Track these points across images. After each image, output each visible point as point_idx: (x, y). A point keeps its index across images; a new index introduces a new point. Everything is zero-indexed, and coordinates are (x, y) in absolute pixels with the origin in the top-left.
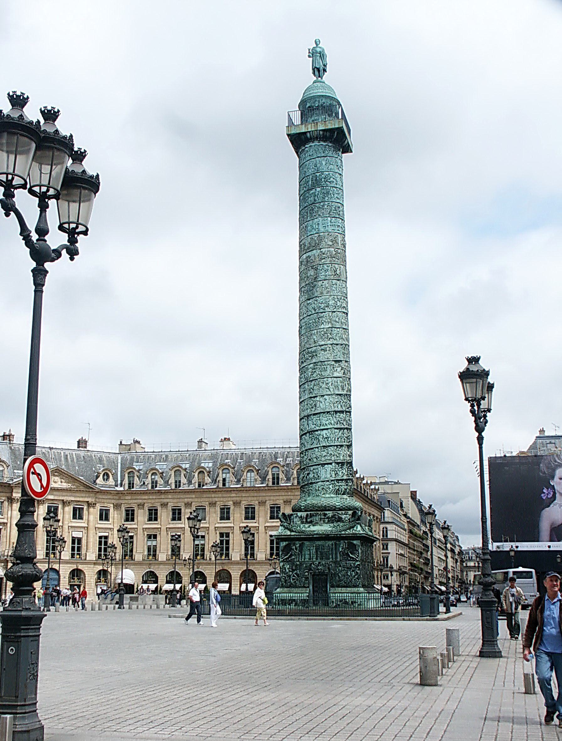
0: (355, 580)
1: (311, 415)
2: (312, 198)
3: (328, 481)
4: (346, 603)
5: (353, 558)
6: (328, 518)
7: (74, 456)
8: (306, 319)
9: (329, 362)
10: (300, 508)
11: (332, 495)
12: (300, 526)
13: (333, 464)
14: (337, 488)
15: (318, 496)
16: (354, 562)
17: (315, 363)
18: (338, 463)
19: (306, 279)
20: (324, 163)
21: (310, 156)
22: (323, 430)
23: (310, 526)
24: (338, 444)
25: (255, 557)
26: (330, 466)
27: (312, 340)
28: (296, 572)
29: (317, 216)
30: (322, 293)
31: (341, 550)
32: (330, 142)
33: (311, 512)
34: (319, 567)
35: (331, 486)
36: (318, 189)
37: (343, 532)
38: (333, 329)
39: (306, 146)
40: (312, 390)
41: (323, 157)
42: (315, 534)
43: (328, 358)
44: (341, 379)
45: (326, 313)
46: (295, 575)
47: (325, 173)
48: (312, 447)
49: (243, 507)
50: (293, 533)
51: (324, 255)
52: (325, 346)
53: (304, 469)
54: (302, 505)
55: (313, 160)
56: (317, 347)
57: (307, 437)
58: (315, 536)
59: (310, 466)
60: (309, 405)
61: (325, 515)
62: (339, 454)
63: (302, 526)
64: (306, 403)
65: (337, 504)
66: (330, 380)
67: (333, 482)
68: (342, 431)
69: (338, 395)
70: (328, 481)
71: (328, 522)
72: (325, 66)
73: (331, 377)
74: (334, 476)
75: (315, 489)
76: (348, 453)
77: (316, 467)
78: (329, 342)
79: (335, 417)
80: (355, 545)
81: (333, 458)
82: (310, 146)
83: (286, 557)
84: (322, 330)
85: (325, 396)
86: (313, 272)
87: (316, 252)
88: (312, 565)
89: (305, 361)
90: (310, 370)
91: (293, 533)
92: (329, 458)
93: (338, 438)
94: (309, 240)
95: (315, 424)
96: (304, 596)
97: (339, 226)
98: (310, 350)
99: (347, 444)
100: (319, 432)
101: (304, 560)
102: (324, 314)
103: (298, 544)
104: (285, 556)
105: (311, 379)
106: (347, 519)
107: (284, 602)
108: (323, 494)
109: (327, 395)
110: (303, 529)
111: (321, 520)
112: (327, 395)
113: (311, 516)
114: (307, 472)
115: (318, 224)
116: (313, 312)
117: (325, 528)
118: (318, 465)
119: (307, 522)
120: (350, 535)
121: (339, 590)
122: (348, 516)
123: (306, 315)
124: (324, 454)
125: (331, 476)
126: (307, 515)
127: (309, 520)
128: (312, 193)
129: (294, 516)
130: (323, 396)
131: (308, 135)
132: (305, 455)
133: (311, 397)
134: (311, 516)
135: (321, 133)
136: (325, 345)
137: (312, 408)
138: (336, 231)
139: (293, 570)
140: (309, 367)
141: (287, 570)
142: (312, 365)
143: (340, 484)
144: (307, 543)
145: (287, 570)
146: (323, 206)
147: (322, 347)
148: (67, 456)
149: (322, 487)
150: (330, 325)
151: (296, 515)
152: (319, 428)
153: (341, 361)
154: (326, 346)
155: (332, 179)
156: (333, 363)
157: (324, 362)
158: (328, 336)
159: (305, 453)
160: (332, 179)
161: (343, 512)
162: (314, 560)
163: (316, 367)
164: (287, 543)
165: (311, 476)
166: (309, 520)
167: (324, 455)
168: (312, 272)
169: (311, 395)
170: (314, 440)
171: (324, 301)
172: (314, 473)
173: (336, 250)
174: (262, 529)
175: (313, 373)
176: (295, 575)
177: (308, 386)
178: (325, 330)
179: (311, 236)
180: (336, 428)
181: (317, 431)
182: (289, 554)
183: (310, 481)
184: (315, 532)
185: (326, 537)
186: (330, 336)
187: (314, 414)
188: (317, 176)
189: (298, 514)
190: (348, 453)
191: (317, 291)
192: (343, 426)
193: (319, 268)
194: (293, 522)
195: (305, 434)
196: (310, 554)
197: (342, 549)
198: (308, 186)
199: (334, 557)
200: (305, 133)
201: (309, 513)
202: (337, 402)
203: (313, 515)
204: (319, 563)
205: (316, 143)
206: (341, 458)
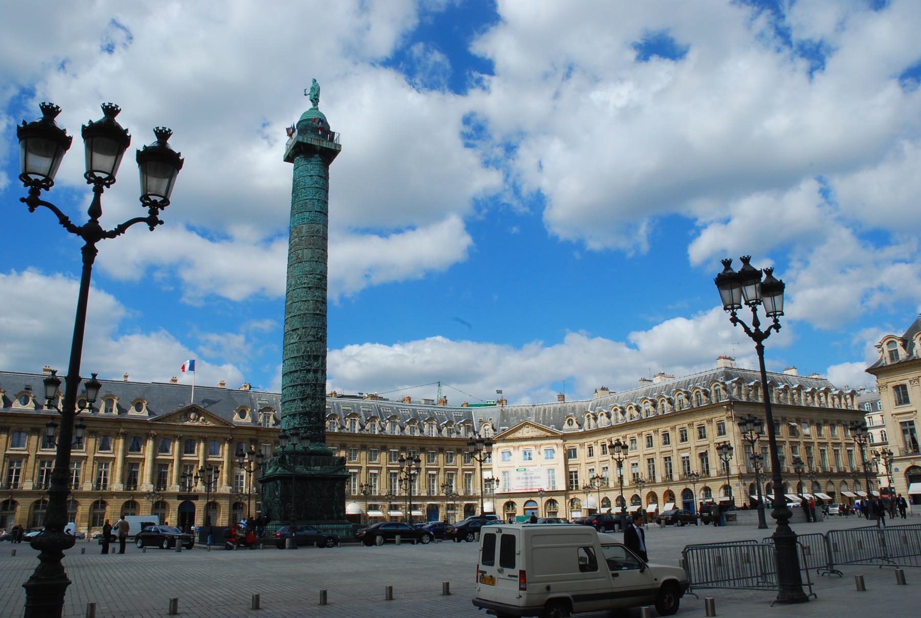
7: (552, 409)
18: (290, 415)
26: (286, 418)
32: (302, 154)
44: (296, 344)
49: (660, 433)
78: (290, 316)
148: (546, 409)
153: (298, 329)
174: (675, 452)
180: (290, 386)
190: (302, 405)
192: (296, 383)
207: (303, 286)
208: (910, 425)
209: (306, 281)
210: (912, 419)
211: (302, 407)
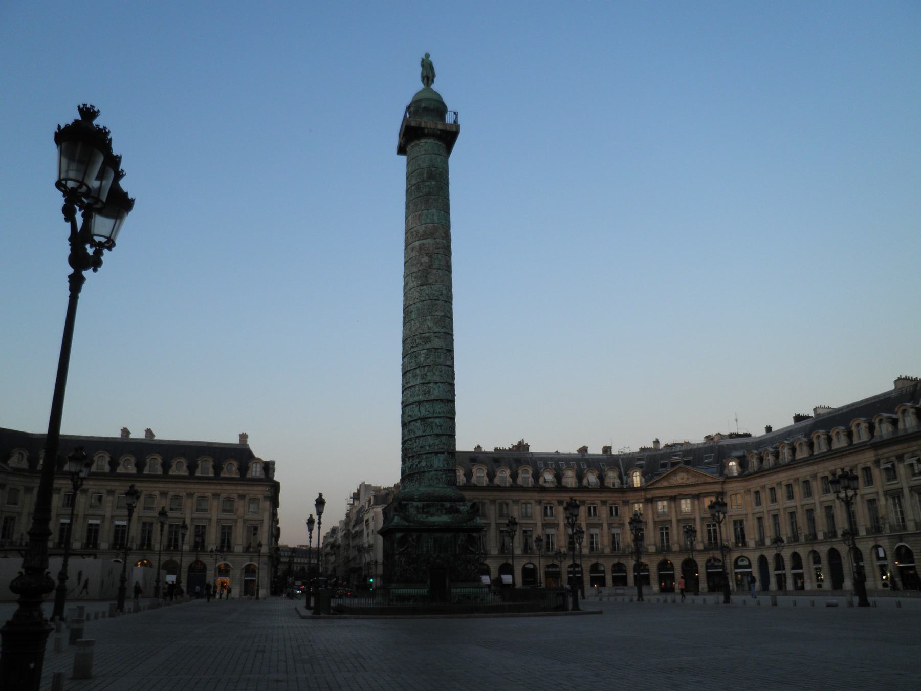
1: (424, 401)
2: (427, 190)
3: (441, 470)
8: (418, 304)
9: (442, 351)
11: (445, 486)
13: (446, 453)
14: (449, 478)
15: (430, 486)
16: (474, 555)
17: (429, 349)
19: (419, 265)
20: (439, 160)
24: (449, 433)
25: (179, 548)
26: (442, 455)
27: (426, 325)
30: (436, 281)
31: (460, 542)
33: (428, 502)
35: (444, 476)
36: (433, 183)
37: (464, 524)
38: (446, 318)
39: (421, 141)
40: (425, 376)
43: (442, 346)
45: (440, 301)
46: (412, 569)
48: (424, 434)
50: (411, 524)
51: (438, 246)
52: (438, 334)
53: (413, 456)
54: (415, 494)
56: (432, 333)
57: (418, 423)
58: (435, 527)
59: (422, 454)
60: (421, 391)
61: (442, 505)
62: (450, 443)
63: (419, 516)
64: (417, 389)
65: (453, 495)
67: (445, 472)
70: (441, 470)
71: (446, 513)
72: (434, 76)
73: (444, 366)
74: (446, 466)
75: (428, 478)
77: (429, 455)
78: (443, 330)
79: (447, 406)
81: (445, 448)
82: (426, 142)
85: (439, 384)
87: (430, 241)
90: (423, 355)
92: (442, 447)
93: (450, 428)
94: (423, 228)
95: (428, 411)
96: (425, 591)
98: (423, 335)
103: (415, 536)
104: (402, 548)
105: (424, 365)
106: (465, 510)
107: (402, 598)
108: (437, 484)
109: (441, 383)
110: (421, 519)
112: (441, 383)
113: (428, 506)
114: (418, 460)
115: (433, 215)
116: (427, 298)
117: (445, 518)
118: (431, 453)
119: (423, 512)
122: (466, 507)
123: (419, 300)
124: (437, 442)
125: (444, 466)
127: (425, 510)
128: (427, 185)
129: (410, 505)
130: (436, 383)
131: (426, 131)
132: (416, 442)
133: (423, 384)
134: (428, 506)
135: (439, 132)
136: (439, 332)
137: (425, 394)
140: (422, 352)
141: (403, 564)
142: (425, 351)
143: (451, 475)
145: (403, 564)
147: (436, 334)
150: (443, 314)
151: (411, 505)
154: (440, 334)
155: (444, 177)
156: (446, 351)
157: (438, 349)
159: (416, 440)
161: (461, 503)
163: (429, 353)
164: (403, 534)
165: (423, 464)
167: (437, 443)
168: (425, 259)
169: (424, 381)
172: (426, 461)
175: (426, 358)
177: (420, 371)
178: (439, 317)
181: (430, 418)
182: (405, 547)
183: (422, 470)
184: (436, 524)
185: (444, 529)
186: (443, 325)
187: (427, 401)
188: (432, 170)
193: (433, 256)
194: (409, 511)
195: (416, 420)
197: (461, 542)
200: (424, 129)
201: (426, 503)
202: (448, 391)
205: (431, 141)
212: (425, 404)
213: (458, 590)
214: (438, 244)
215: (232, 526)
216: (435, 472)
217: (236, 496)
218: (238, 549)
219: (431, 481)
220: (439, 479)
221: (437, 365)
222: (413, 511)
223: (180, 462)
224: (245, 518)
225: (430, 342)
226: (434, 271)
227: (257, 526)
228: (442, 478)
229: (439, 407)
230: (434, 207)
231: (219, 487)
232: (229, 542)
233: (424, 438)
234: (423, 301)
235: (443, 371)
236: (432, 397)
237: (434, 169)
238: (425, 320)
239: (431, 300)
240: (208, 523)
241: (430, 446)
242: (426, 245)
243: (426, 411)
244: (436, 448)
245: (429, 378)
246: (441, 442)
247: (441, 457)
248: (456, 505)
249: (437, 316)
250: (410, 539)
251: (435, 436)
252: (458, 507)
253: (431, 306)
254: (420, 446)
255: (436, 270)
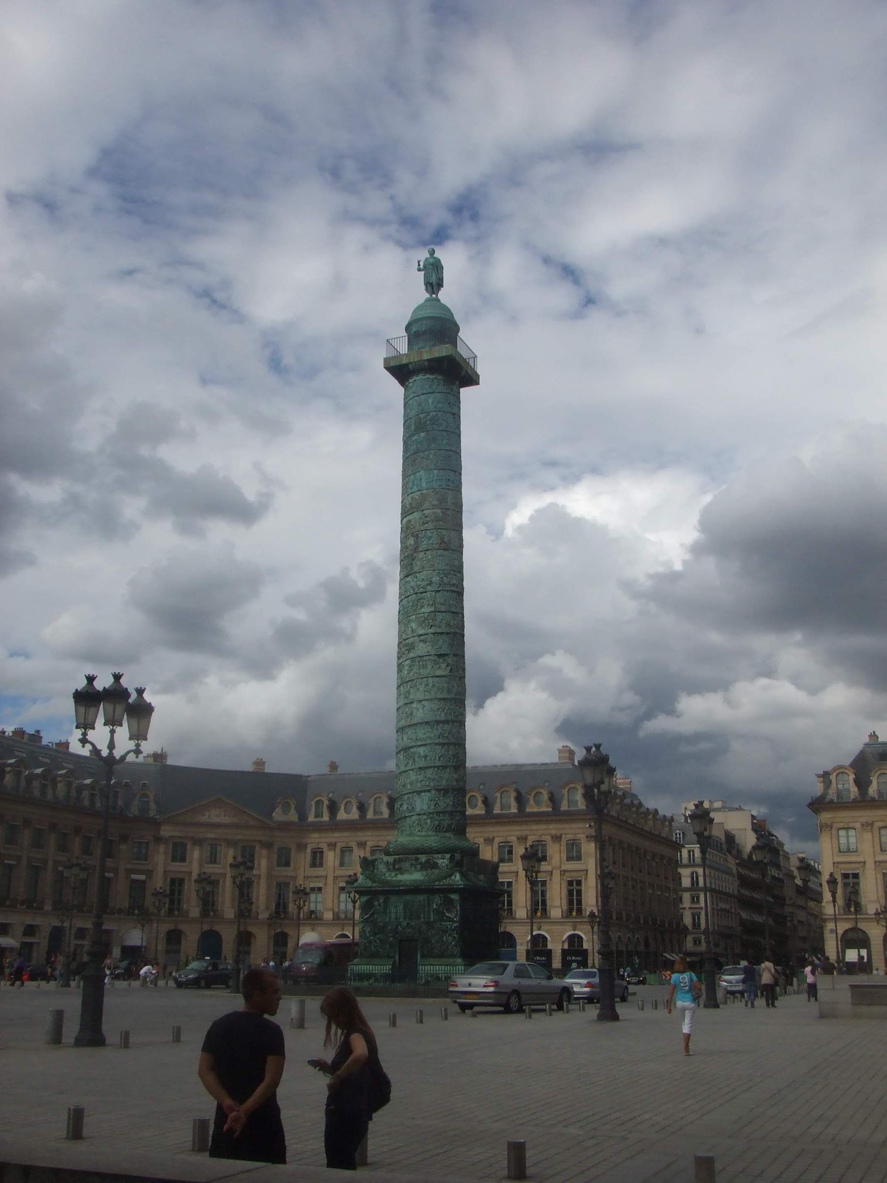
0: (452, 947)
3: (424, 814)
4: (438, 978)
5: (450, 918)
6: (421, 863)
10: (390, 851)
11: (430, 833)
12: (385, 874)
13: (433, 792)
14: (437, 823)
15: (411, 834)
16: (451, 923)
20: (430, 401)
21: (414, 393)
22: (420, 746)
23: (396, 875)
24: (440, 764)
26: (428, 794)
28: (378, 936)
29: (419, 469)
34: (408, 930)
35: (429, 821)
36: (422, 435)
41: (430, 393)
42: (403, 886)
43: (428, 652)
45: (428, 593)
46: (377, 940)
47: (431, 414)
50: (374, 885)
51: (427, 519)
55: (416, 398)
56: (416, 638)
58: (401, 888)
61: (417, 859)
65: (434, 845)
66: (430, 680)
67: (431, 816)
68: (446, 747)
69: (440, 699)
70: (424, 814)
71: (422, 869)
73: (433, 677)
74: (432, 807)
76: (456, 776)
77: (410, 795)
78: (432, 630)
80: (452, 901)
81: (432, 784)
82: (415, 380)
83: (367, 916)
84: (422, 615)
86: (413, 541)
87: (417, 515)
88: (399, 927)
89: (401, 656)
90: (407, 668)
91: (374, 885)
93: (440, 757)
95: (410, 739)
96: (386, 969)
97: (449, 480)
98: (407, 641)
99: (454, 764)
100: (414, 750)
101: (389, 920)
102: (424, 594)
104: (367, 915)
105: (407, 680)
106: (444, 865)
107: (361, 977)
109: (426, 700)
111: (411, 866)
112: (426, 700)
113: (400, 861)
114: (400, 803)
115: (421, 479)
116: (412, 591)
117: (415, 876)
118: (413, 792)
120: (445, 887)
121: (432, 960)
122: (445, 860)
124: (420, 778)
126: (395, 860)
127: (397, 867)
129: (379, 861)
130: (420, 701)
131: (410, 367)
134: (400, 861)
135: (426, 363)
136: (425, 634)
137: (408, 717)
138: (444, 486)
139: (375, 934)
142: (409, 660)
144: (393, 898)
146: (428, 456)
147: (422, 637)
149: (417, 822)
150: (432, 609)
152: (416, 745)
153: (447, 655)
155: (441, 421)
156: (436, 657)
157: (423, 656)
158: (429, 623)
160: (441, 421)
161: (440, 856)
162: (402, 920)
163: (412, 664)
165: (405, 807)
166: (397, 867)
167: (419, 780)
170: (409, 760)
171: (425, 578)
172: (407, 804)
173: (444, 510)
175: (410, 671)
176: (377, 940)
177: (404, 689)
179: (411, 495)
181: (412, 747)
182: (371, 913)
185: (415, 889)
187: (410, 726)
188: (420, 417)
189: (384, 859)
190: (456, 776)
191: (416, 565)
192: (447, 741)
193: (420, 535)
194: (378, 869)
196: (397, 913)
197: (437, 905)
198: (411, 430)
199: (426, 916)
200: (406, 365)
201: (397, 857)
202: (439, 709)
203: (402, 860)
204: (408, 924)
206: (444, 782)
207: (452, 589)
208: (853, 878)
209: (455, 582)
210: (858, 871)
211: (457, 780)
212: (407, 730)
213: (427, 969)
214: (426, 517)
215: (546, 881)
216: (417, 817)
217: (548, 838)
218: (556, 913)
219: (412, 829)
220: (421, 826)
221: (422, 678)
222: (382, 868)
223: (473, 795)
224: (562, 869)
225: (414, 648)
226: (421, 555)
227: (579, 879)
228: (426, 823)
229: (424, 731)
230: (422, 468)
231: (524, 827)
232: (544, 903)
233: (406, 773)
234: (408, 596)
235: (431, 685)
236: (415, 721)
237: (424, 415)
238: (409, 622)
239: (417, 593)
240: (514, 879)
241: (411, 784)
242: (412, 523)
243: (408, 739)
244: (419, 785)
245: (411, 697)
246: (425, 777)
247: (426, 796)
248: (433, 858)
249: (423, 613)
250: (376, 903)
251: (418, 770)
252: (435, 860)
253: (416, 602)
254: (402, 784)
255: (423, 553)
